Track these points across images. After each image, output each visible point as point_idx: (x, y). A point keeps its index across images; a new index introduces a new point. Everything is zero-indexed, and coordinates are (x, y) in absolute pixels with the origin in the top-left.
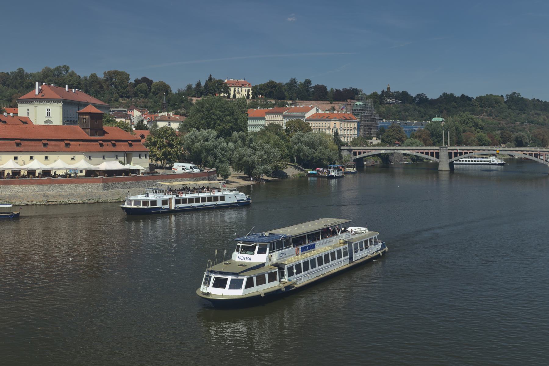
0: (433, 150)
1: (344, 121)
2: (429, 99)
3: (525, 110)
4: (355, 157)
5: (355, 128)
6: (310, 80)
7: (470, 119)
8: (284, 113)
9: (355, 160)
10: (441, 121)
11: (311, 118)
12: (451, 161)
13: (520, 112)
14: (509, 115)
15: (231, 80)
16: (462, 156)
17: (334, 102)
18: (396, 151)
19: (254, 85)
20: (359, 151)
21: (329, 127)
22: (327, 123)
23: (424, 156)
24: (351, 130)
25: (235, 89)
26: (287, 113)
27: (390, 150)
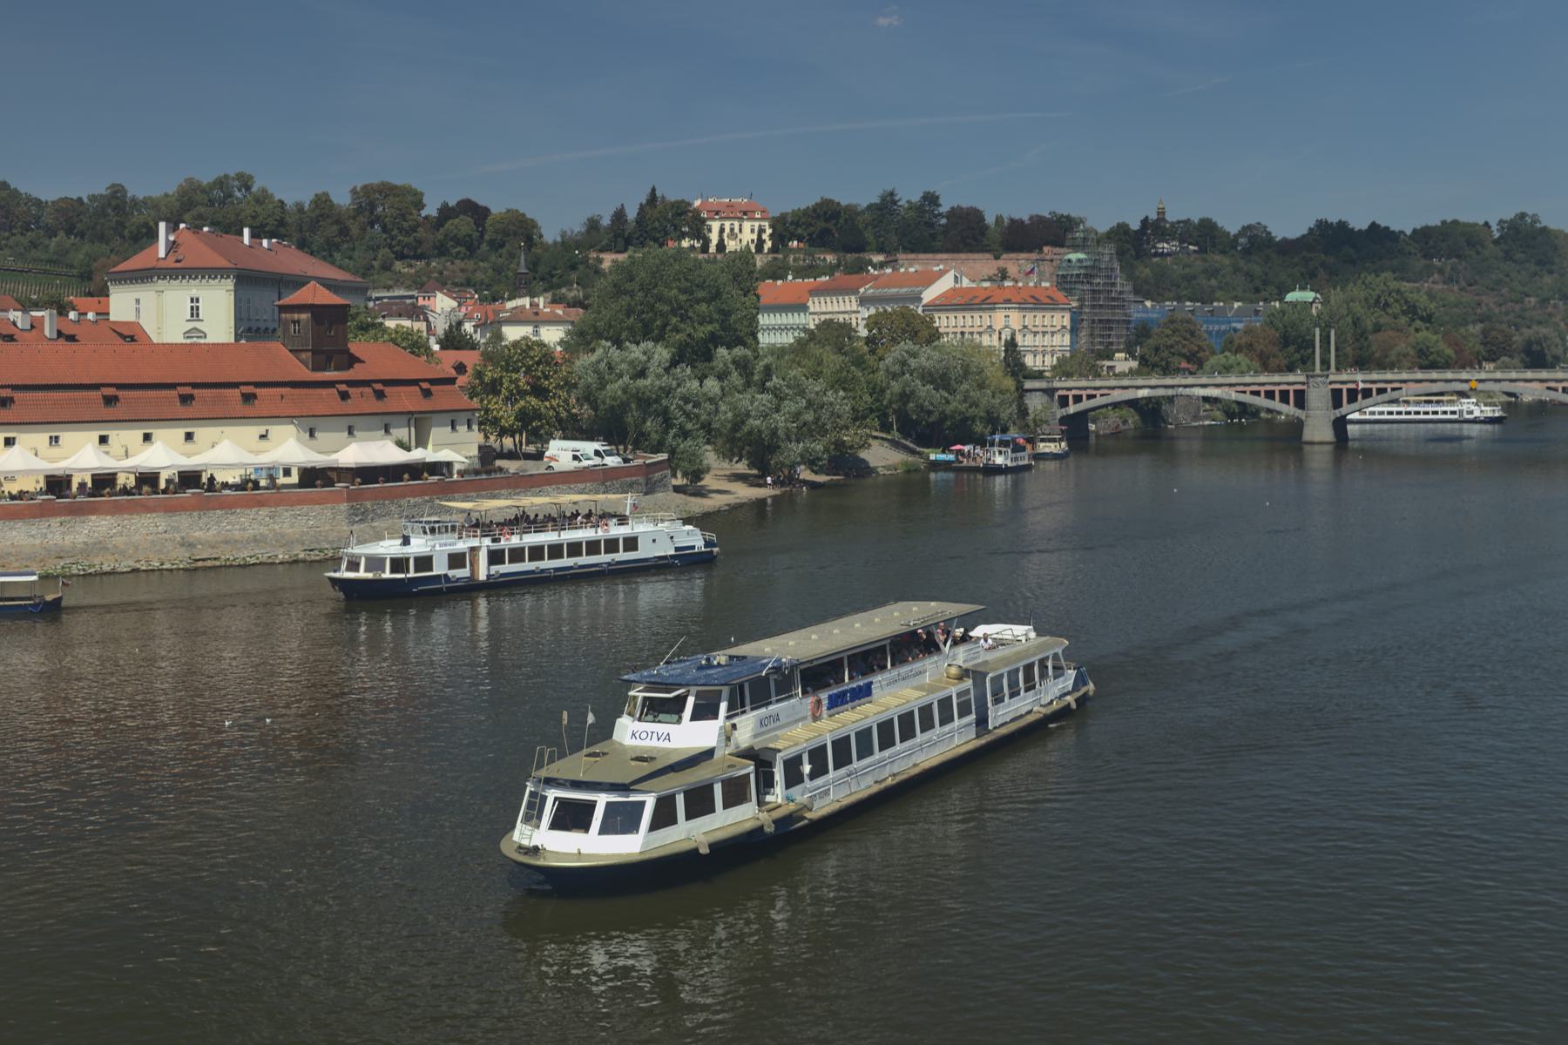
0: (1288, 384)
1: (1034, 309)
2: (1277, 239)
3: (1553, 263)
4: (1064, 412)
5: (1064, 327)
6: (937, 194)
7: (1394, 294)
8: (862, 290)
9: (1064, 420)
10: (1311, 300)
11: (938, 302)
12: (1339, 415)
13: (1538, 268)
14: (1507, 279)
15: (711, 200)
17: (1005, 256)
18: (1181, 389)
19: (777, 214)
21: (990, 327)
22: (985, 315)
23: (1261, 401)
24: (1053, 333)
25: (722, 225)
26: (871, 291)
27: (1166, 387)
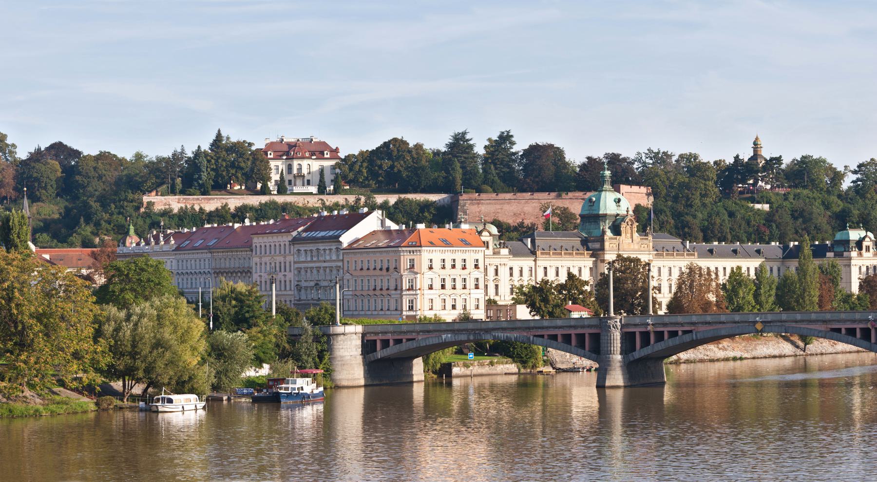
16: (662, 342)
17: (570, 194)
20: (381, 337)
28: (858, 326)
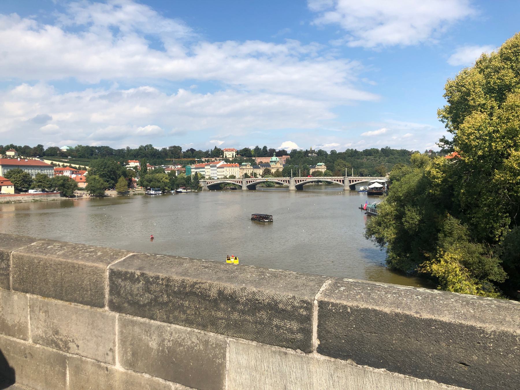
8: (211, 165)
9: (208, 186)
28: (282, 180)
